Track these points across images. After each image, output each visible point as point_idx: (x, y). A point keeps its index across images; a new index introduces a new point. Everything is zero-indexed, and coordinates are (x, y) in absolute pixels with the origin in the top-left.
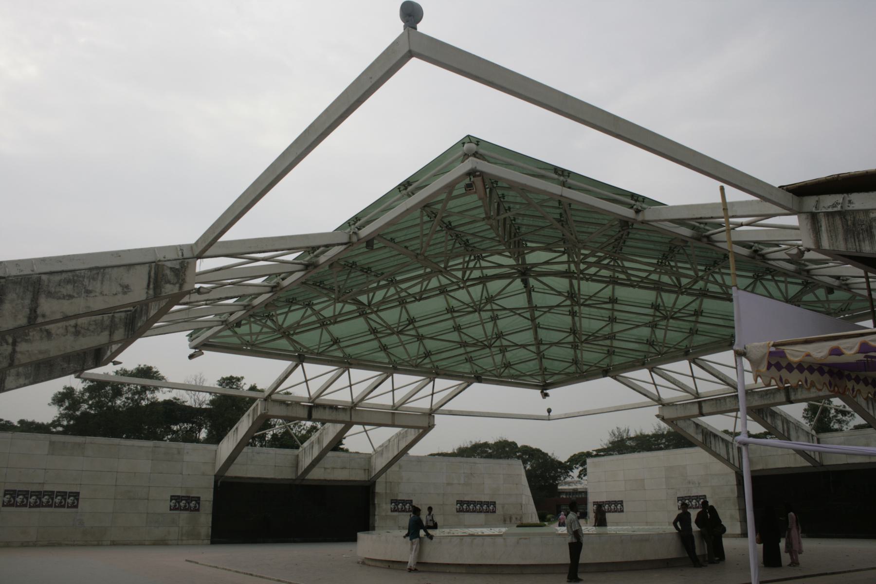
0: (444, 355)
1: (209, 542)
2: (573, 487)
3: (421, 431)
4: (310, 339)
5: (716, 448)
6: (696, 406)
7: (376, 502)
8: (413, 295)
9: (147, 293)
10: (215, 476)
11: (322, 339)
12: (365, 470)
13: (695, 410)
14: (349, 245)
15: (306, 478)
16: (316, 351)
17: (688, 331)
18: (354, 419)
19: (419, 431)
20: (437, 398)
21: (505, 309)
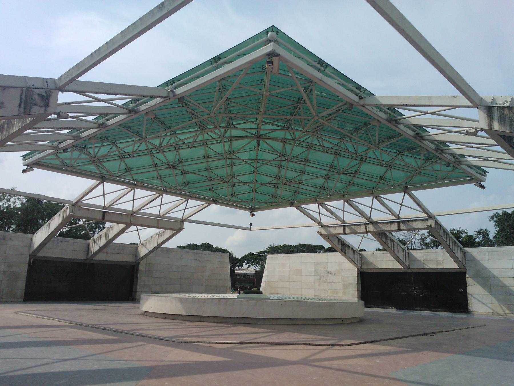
0: (196, 185)
1: (23, 300)
3: (174, 231)
4: (114, 166)
5: (348, 254)
6: (342, 228)
7: (139, 276)
8: (187, 144)
9: (19, 110)
10: (30, 255)
11: (120, 168)
12: (133, 255)
13: (341, 230)
14: (167, 98)
15: (93, 259)
16: (116, 175)
17: (347, 183)
18: (133, 222)
19: (173, 232)
20: (188, 212)
21: (240, 159)
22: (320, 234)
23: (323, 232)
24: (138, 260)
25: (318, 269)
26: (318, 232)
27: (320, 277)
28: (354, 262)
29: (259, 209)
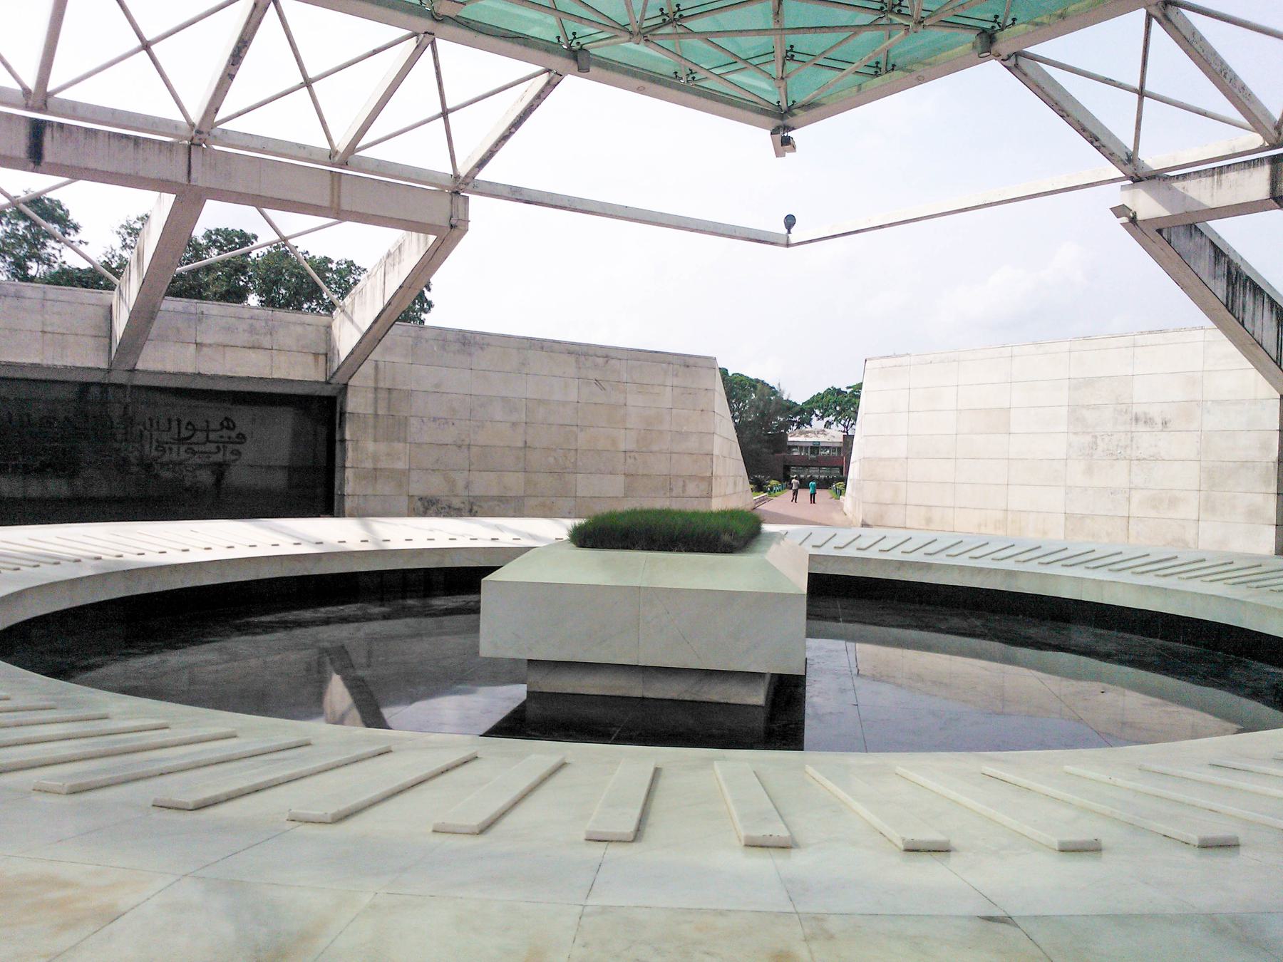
2: (815, 439)
7: (348, 436)
12: (316, 355)
22: (1125, 220)
23: (1147, 205)
24: (334, 374)
25: (1088, 407)
26: (1119, 211)
27: (1096, 437)
28: (1276, 363)
29: (814, 108)
